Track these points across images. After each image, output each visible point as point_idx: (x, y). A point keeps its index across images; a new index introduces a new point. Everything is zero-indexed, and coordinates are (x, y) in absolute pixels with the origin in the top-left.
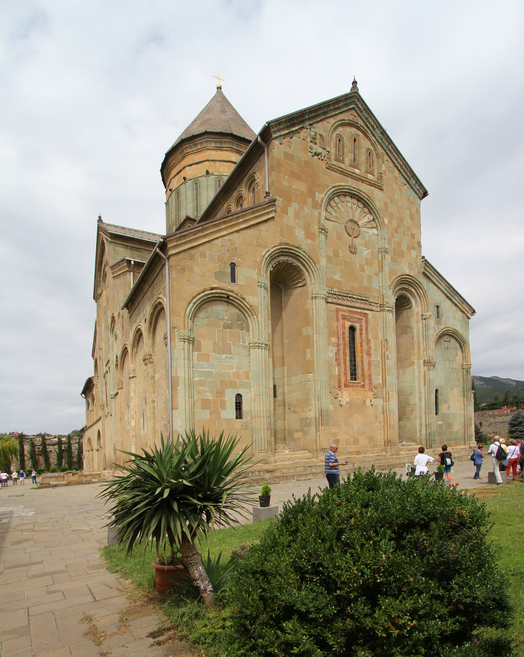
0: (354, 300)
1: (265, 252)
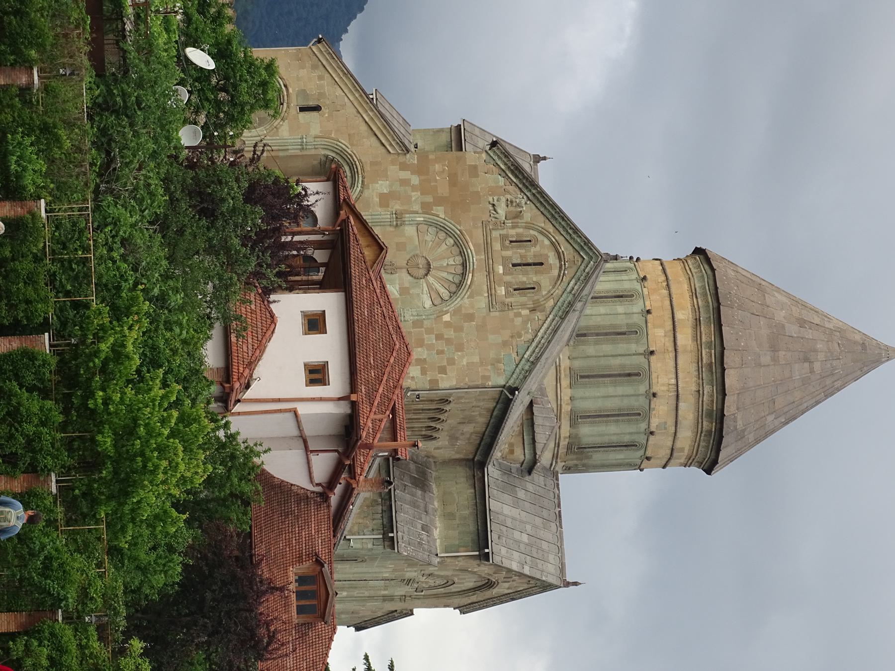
1: (344, 143)
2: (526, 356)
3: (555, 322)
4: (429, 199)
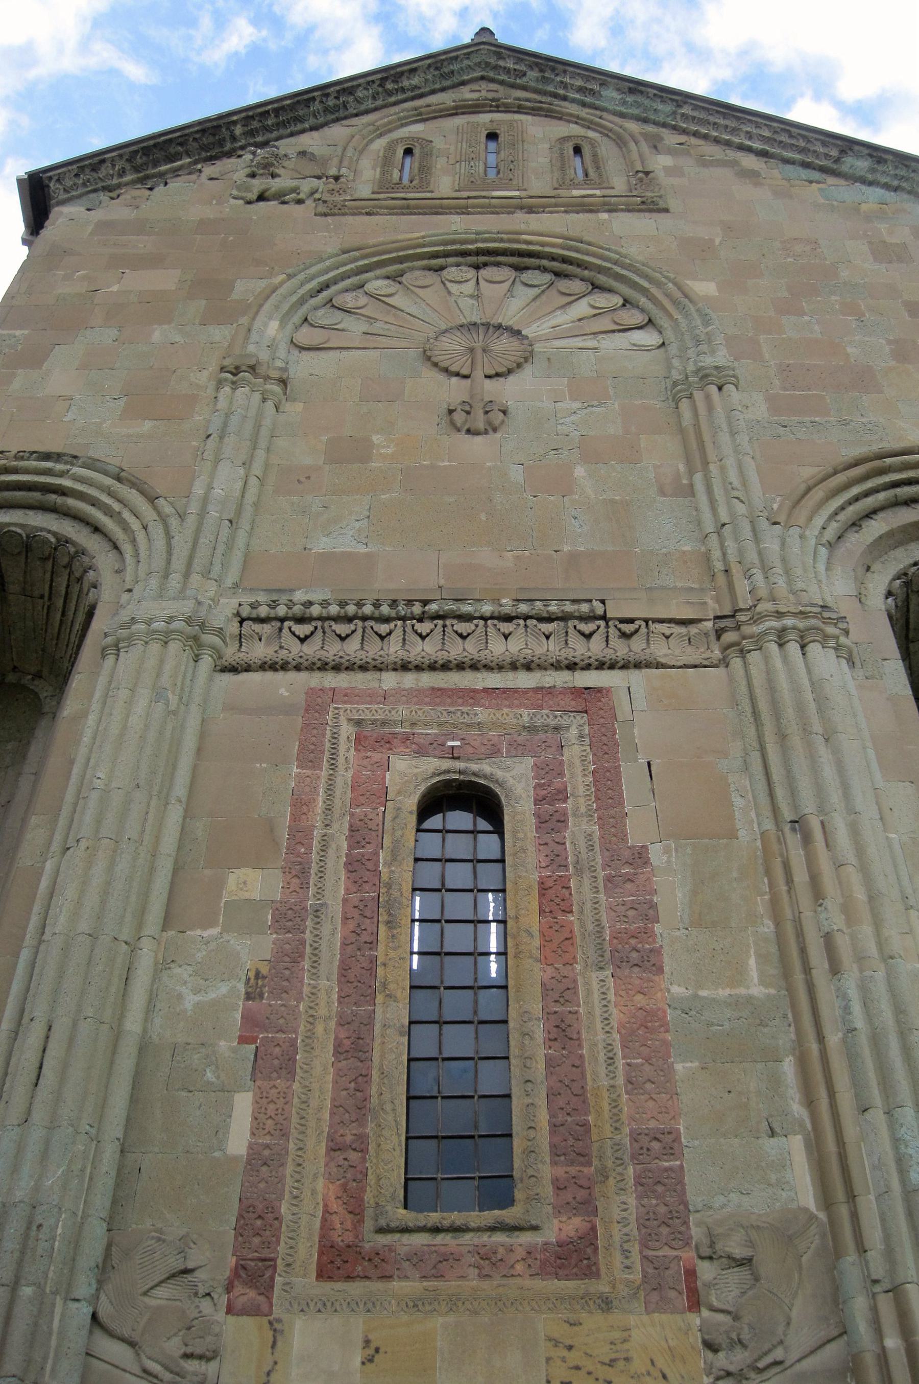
0: (463, 627)
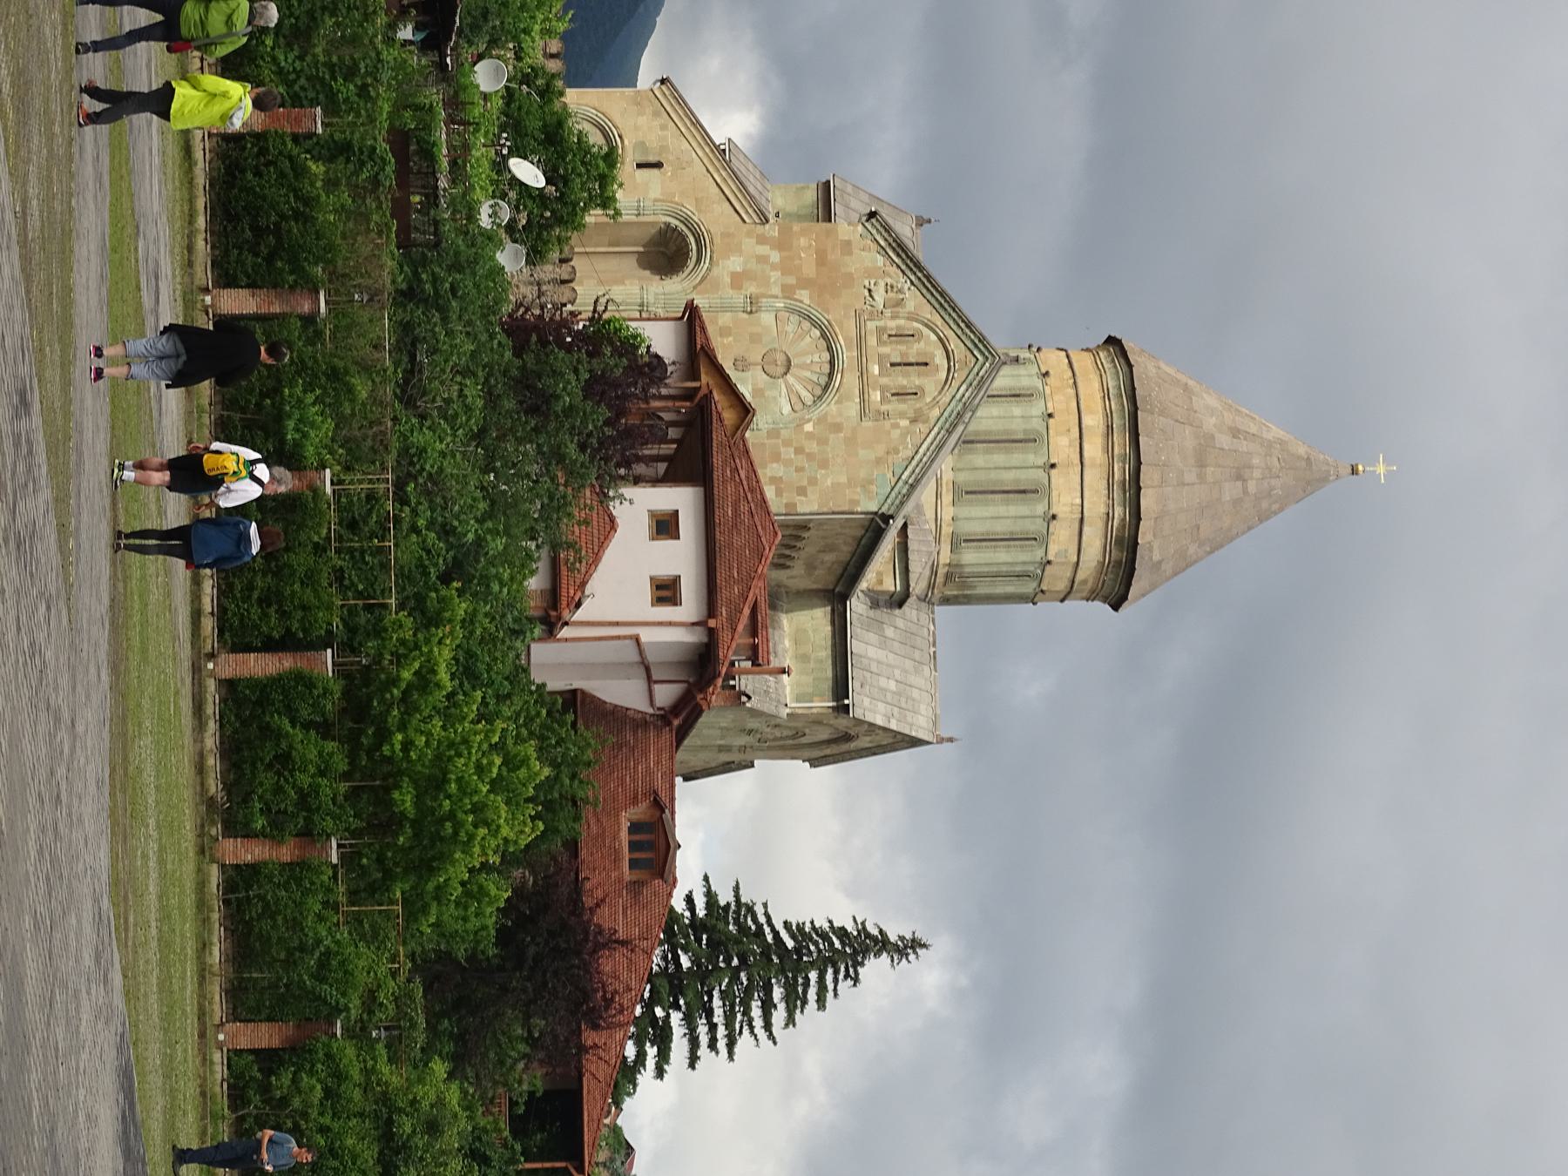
1: (690, 208)
2: (904, 477)
3: (940, 436)
4: (792, 280)
